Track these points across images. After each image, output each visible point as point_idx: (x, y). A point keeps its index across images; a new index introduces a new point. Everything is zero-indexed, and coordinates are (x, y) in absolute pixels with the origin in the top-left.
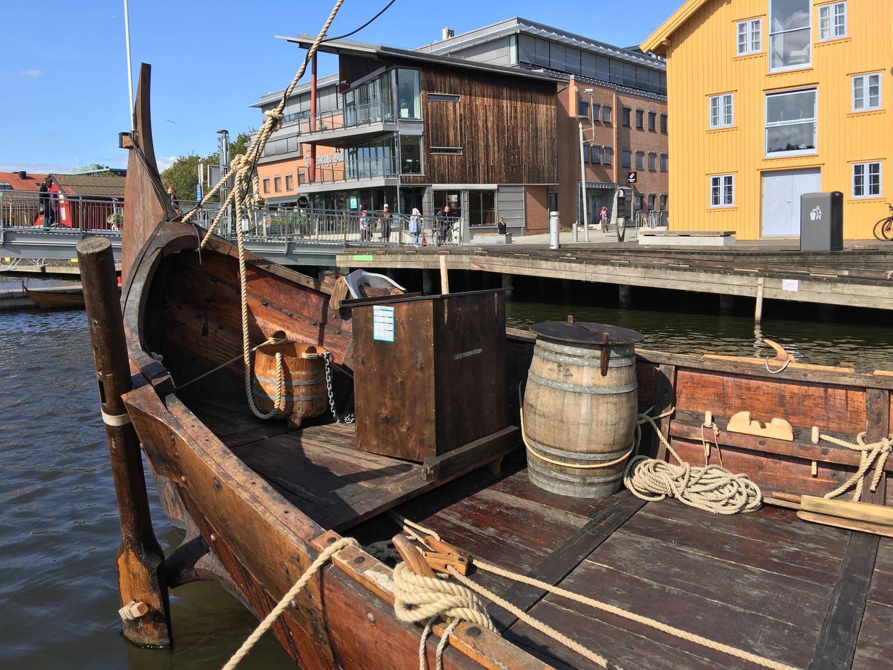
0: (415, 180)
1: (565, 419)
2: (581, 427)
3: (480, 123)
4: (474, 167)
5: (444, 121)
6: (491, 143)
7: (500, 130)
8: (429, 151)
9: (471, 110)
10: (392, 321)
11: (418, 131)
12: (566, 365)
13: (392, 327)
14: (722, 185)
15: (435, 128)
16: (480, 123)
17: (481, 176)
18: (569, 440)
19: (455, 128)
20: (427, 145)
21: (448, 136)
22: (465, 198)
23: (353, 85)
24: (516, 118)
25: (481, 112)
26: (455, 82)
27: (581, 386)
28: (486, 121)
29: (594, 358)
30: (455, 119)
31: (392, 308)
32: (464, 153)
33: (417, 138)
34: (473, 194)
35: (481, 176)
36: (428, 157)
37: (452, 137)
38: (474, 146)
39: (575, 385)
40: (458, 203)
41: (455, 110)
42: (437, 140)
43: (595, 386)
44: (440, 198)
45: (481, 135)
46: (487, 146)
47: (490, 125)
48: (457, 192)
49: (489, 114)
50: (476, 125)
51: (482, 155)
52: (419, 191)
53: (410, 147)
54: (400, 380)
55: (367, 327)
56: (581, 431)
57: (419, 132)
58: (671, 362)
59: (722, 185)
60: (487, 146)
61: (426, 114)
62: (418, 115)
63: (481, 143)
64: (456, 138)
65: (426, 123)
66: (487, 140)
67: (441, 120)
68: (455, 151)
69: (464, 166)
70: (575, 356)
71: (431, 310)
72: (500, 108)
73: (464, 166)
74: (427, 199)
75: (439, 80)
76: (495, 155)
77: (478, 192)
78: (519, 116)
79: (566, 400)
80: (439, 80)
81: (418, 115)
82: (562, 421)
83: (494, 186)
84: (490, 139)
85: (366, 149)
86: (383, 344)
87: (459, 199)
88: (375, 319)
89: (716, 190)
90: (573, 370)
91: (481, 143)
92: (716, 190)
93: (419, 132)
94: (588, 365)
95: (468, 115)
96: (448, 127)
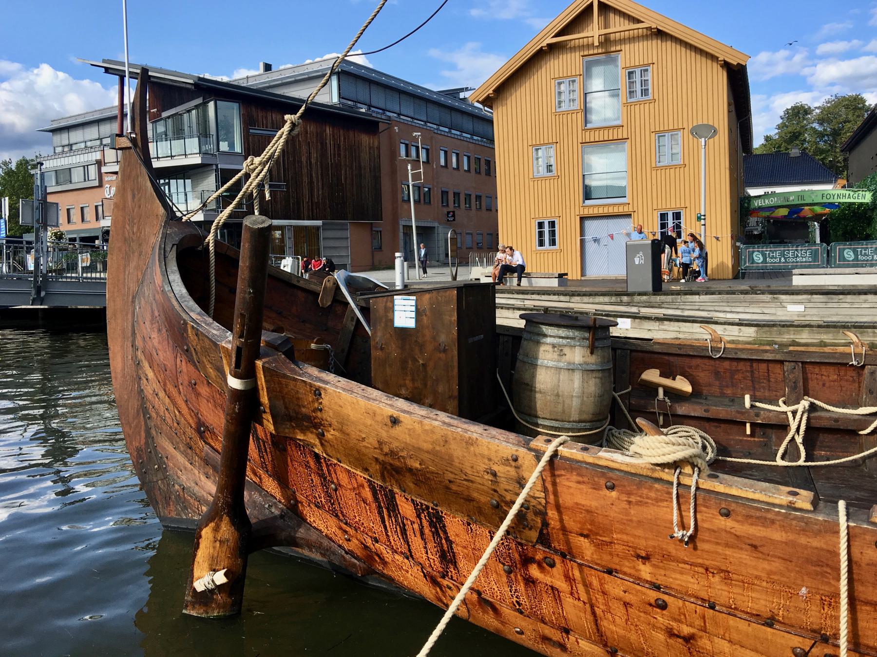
1: (560, 393)
2: (574, 399)
3: (304, 159)
6: (315, 179)
10: (414, 309)
12: (560, 346)
13: (413, 315)
14: (546, 229)
16: (304, 159)
17: (306, 213)
18: (564, 412)
22: (288, 234)
23: (165, 114)
24: (339, 155)
25: (304, 148)
27: (574, 364)
28: (309, 158)
29: (584, 339)
31: (414, 298)
32: (288, 188)
34: (297, 229)
35: (306, 213)
39: (569, 363)
40: (282, 240)
43: (586, 363)
45: (305, 171)
46: (311, 182)
47: (313, 161)
48: (280, 228)
49: (312, 151)
50: (300, 162)
51: (306, 192)
54: (421, 362)
55: (387, 316)
56: (574, 403)
58: (627, 347)
59: (546, 229)
60: (311, 182)
63: (306, 179)
66: (311, 176)
70: (567, 338)
71: (455, 298)
75: (260, 115)
78: (342, 153)
79: (561, 377)
80: (260, 115)
82: (558, 395)
83: (319, 223)
85: (181, 182)
86: (404, 331)
87: (282, 234)
88: (396, 308)
89: (541, 234)
90: (566, 350)
91: (306, 179)
92: (541, 234)
94: (580, 346)
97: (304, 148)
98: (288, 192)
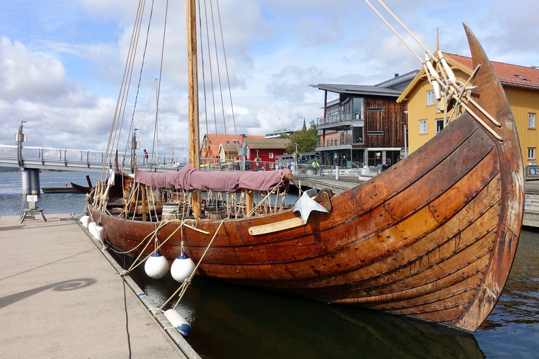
0: (359, 146)
4: (389, 140)
5: (375, 120)
6: (398, 129)
8: (366, 133)
15: (370, 124)
16: (393, 120)
19: (380, 123)
20: (366, 131)
21: (376, 127)
25: (394, 115)
28: (396, 119)
30: (380, 119)
32: (384, 134)
33: (362, 127)
35: (393, 144)
36: (366, 136)
37: (378, 127)
38: (389, 131)
41: (380, 115)
42: (371, 128)
44: (371, 154)
45: (393, 125)
46: (396, 130)
50: (391, 121)
51: (393, 134)
52: (363, 151)
53: (357, 131)
57: (362, 125)
60: (396, 130)
61: (366, 117)
62: (362, 118)
63: (393, 129)
64: (380, 127)
65: (365, 121)
66: (397, 127)
67: (373, 119)
68: (381, 133)
69: (384, 139)
73: (384, 139)
74: (366, 154)
77: (391, 151)
81: (362, 118)
84: (398, 127)
91: (393, 129)
93: (362, 125)
95: (387, 116)
96: (376, 123)
97: (394, 115)
98: (384, 135)
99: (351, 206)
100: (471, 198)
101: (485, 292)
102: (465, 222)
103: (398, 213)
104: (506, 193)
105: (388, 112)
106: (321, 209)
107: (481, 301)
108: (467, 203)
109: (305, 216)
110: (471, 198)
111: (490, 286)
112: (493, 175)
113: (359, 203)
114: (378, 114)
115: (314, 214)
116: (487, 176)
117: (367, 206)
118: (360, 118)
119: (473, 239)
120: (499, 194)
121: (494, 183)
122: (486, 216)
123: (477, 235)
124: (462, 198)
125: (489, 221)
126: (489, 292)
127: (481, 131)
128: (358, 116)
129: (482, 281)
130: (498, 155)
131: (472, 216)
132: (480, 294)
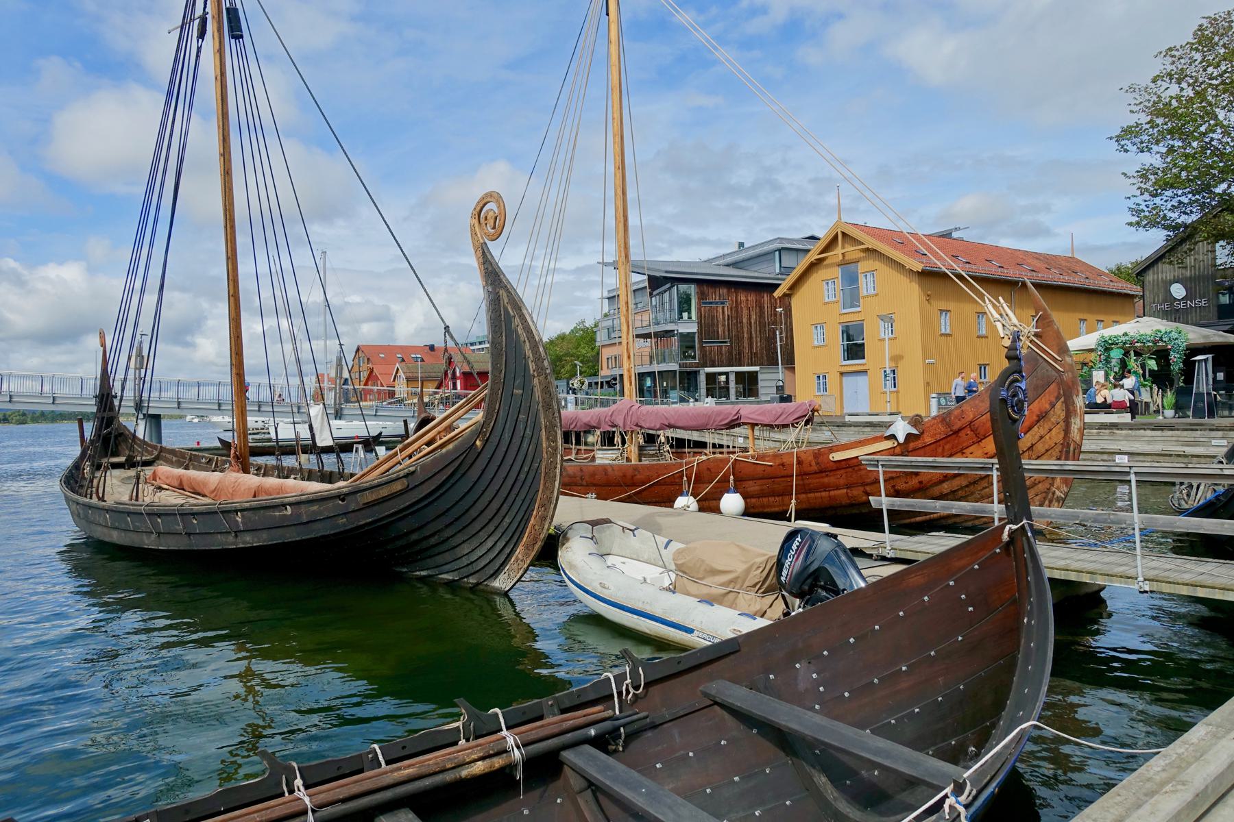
7: (762, 325)
9: (737, 311)
11: (692, 328)
15: (708, 328)
16: (745, 321)
25: (745, 312)
26: (723, 291)
38: (739, 338)
45: (745, 329)
46: (751, 338)
50: (742, 322)
51: (746, 344)
60: (751, 338)
63: (746, 336)
72: (762, 308)
73: (731, 353)
76: (758, 344)
91: (746, 336)
97: (745, 312)
99: (942, 428)
100: (1042, 416)
101: (1054, 493)
102: (1037, 437)
103: (982, 432)
104: (1069, 412)
105: (736, 308)
106: (915, 431)
107: (1051, 502)
108: (1038, 421)
109: (901, 439)
110: (1042, 416)
111: (1058, 488)
112: (1058, 398)
113: (949, 425)
114: (720, 310)
115: (909, 437)
116: (1053, 400)
117: (955, 428)
118: (690, 318)
119: (1043, 450)
120: (1064, 413)
121: (1059, 405)
122: (1053, 432)
123: (1047, 447)
124: (1035, 418)
125: (1057, 435)
126: (1058, 493)
127: (1045, 364)
128: (685, 315)
129: (1052, 485)
130: (1061, 383)
131: (1042, 432)
132: (1050, 495)
